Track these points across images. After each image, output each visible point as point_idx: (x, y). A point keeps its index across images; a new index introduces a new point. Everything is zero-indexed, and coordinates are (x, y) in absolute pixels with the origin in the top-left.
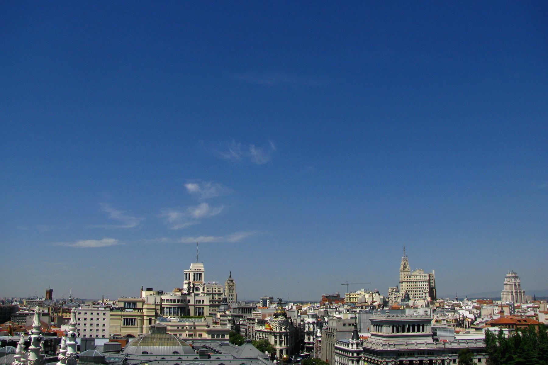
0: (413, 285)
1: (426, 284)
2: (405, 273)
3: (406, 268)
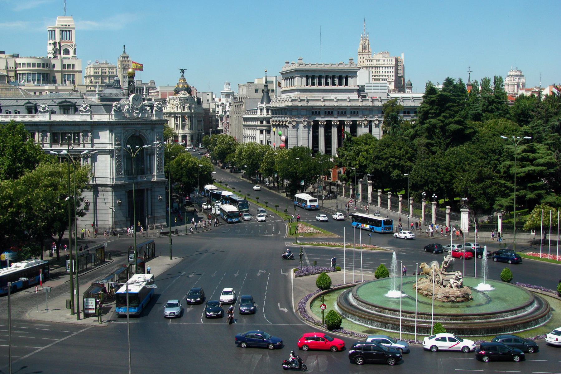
0: (374, 72)
1: (392, 70)
2: (365, 56)
3: (366, 49)
